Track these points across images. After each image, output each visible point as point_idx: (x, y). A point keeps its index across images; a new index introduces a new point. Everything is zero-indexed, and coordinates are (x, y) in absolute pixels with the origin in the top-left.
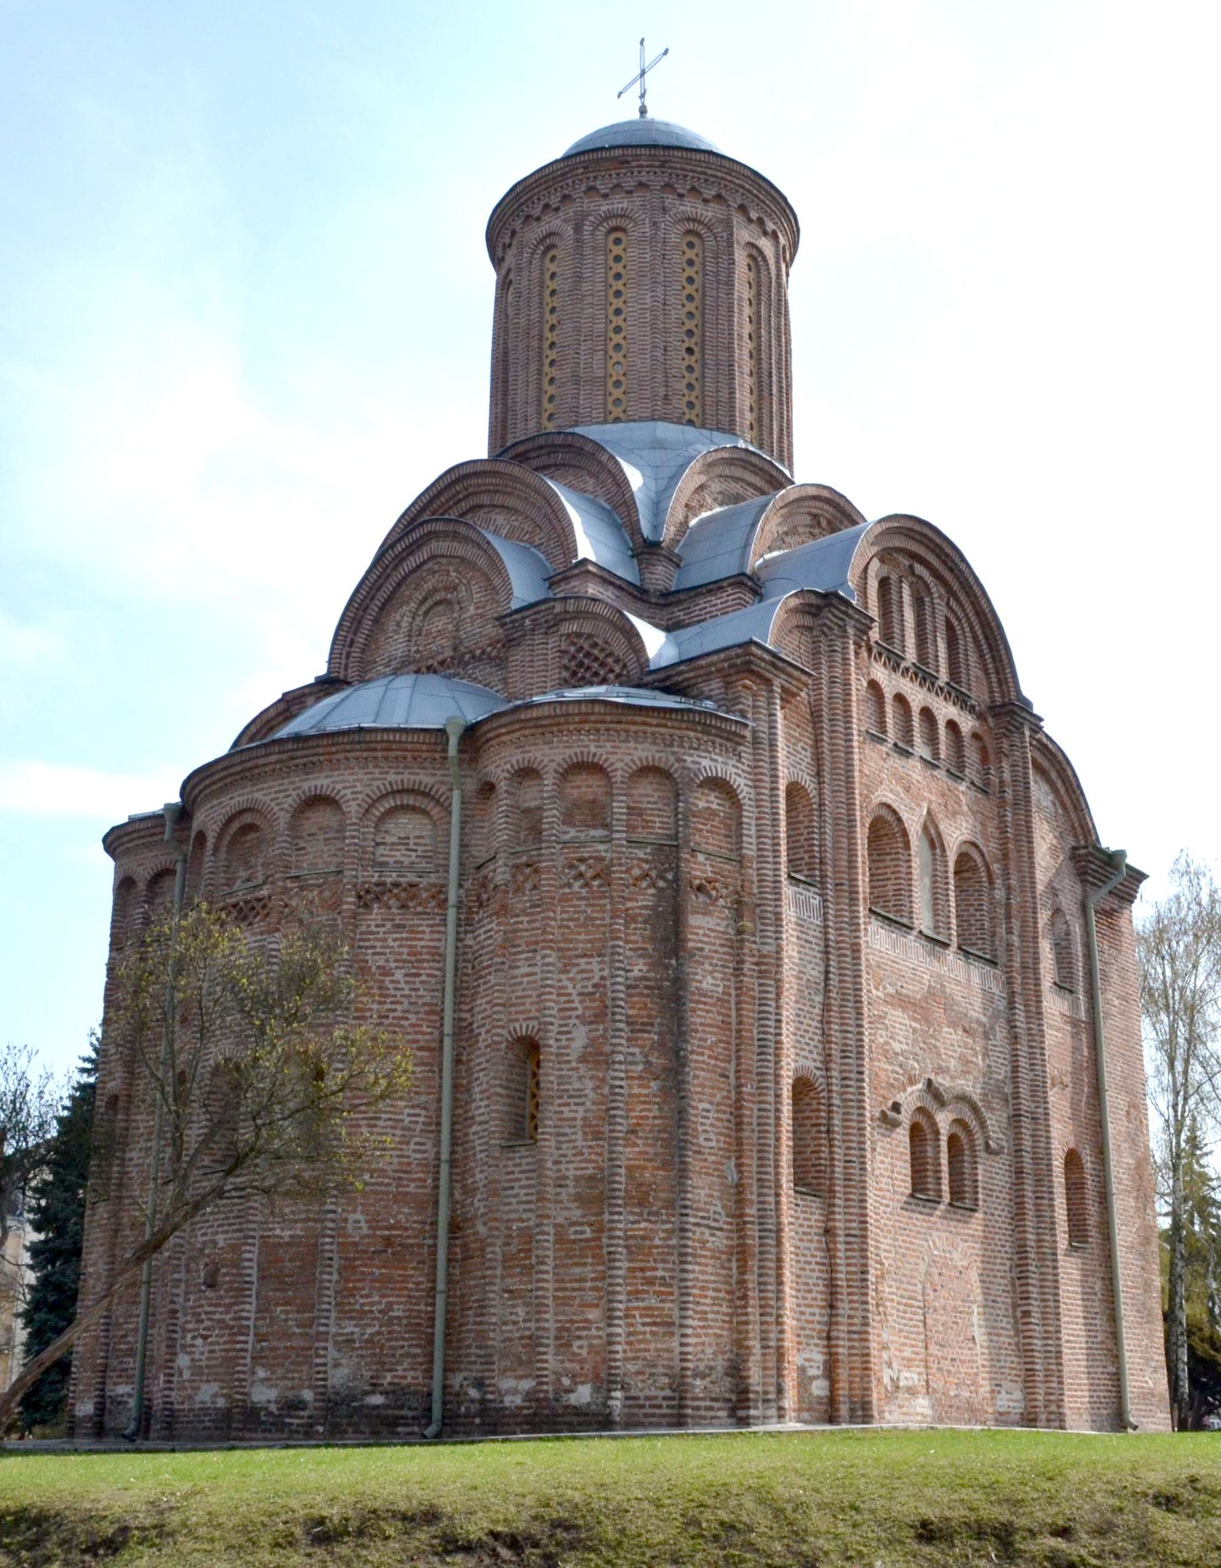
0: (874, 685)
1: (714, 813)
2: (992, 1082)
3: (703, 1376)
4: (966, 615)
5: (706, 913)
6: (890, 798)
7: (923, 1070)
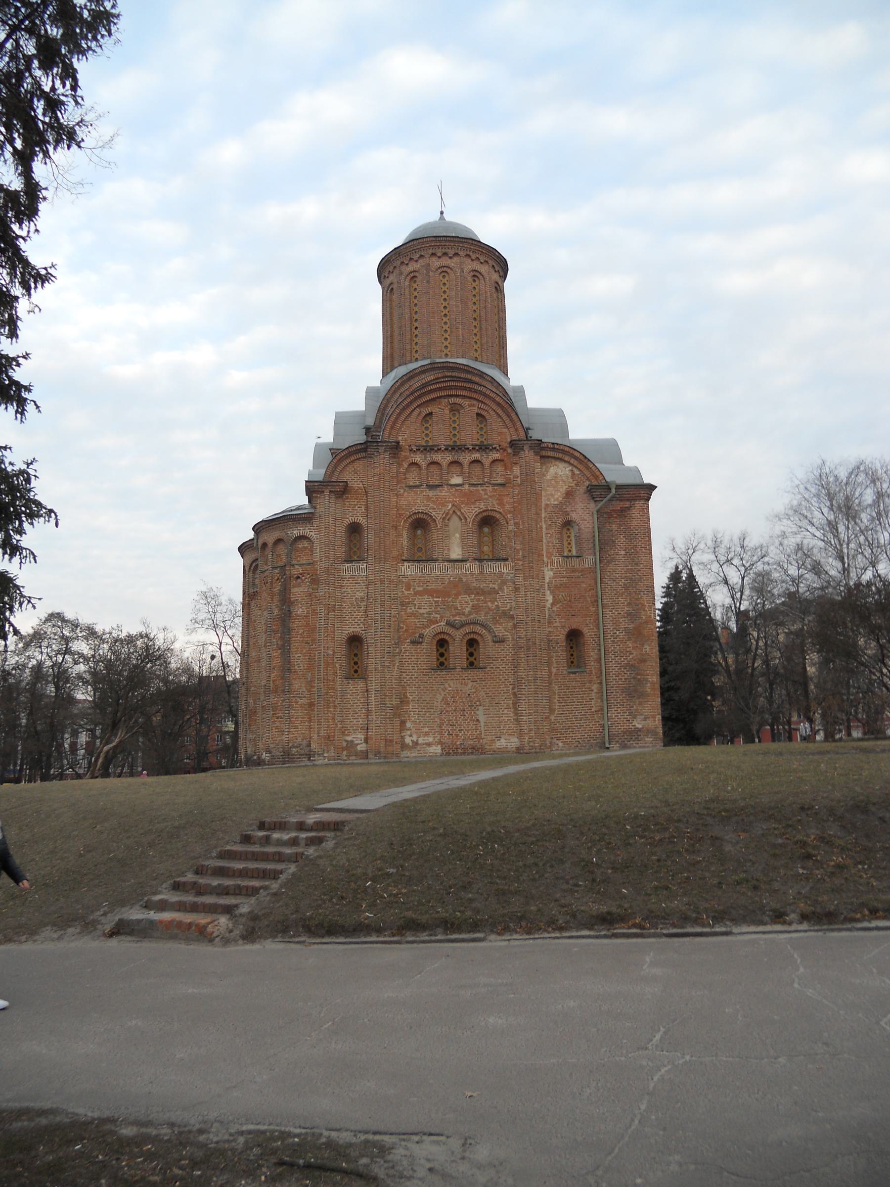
1: (306, 548)
5: (299, 586)
7: (442, 617)
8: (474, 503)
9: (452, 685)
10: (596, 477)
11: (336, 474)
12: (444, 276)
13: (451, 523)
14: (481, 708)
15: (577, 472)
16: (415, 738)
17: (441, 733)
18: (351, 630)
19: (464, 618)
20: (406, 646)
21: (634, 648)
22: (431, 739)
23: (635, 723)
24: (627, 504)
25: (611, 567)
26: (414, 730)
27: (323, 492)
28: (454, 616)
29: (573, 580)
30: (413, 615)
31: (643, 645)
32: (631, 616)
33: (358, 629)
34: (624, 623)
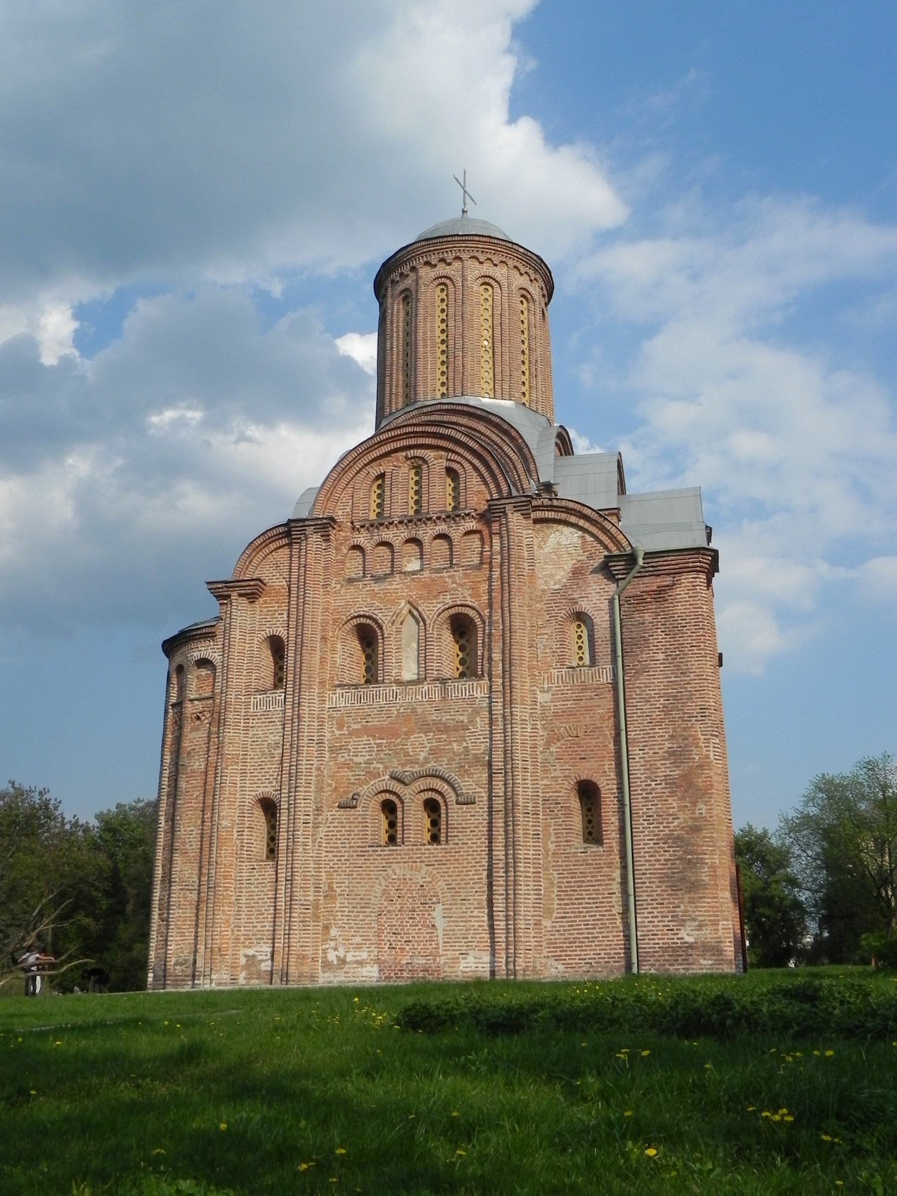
0: (357, 547)
2: (470, 757)
3: (181, 964)
4: (464, 458)
6: (364, 610)
7: (386, 768)
8: (436, 597)
9: (398, 871)
10: (617, 543)
11: (251, 568)
12: (442, 290)
13: (404, 629)
14: (439, 907)
15: (589, 539)
16: (341, 953)
17: (378, 945)
18: (260, 790)
19: (416, 768)
20: (331, 814)
21: (681, 808)
22: (365, 955)
23: (683, 934)
24: (668, 580)
25: (643, 679)
26: (340, 940)
27: (229, 596)
28: (404, 765)
29: (582, 703)
30: (347, 766)
31: (695, 804)
32: (677, 755)
33: (268, 789)
34: (665, 769)
